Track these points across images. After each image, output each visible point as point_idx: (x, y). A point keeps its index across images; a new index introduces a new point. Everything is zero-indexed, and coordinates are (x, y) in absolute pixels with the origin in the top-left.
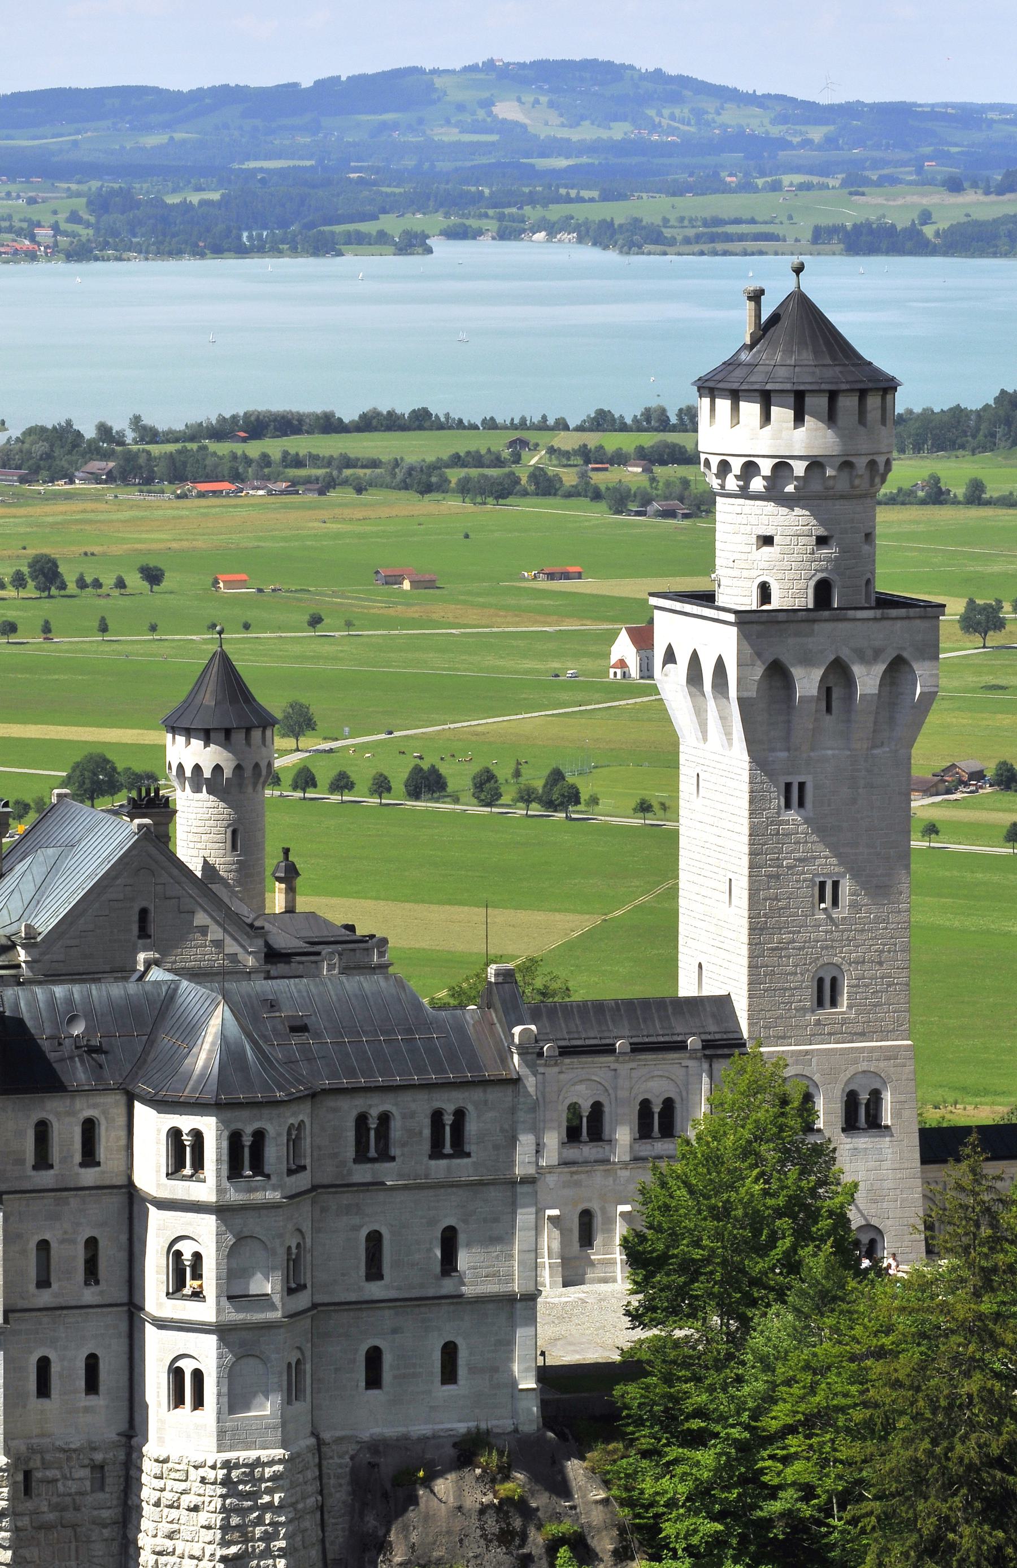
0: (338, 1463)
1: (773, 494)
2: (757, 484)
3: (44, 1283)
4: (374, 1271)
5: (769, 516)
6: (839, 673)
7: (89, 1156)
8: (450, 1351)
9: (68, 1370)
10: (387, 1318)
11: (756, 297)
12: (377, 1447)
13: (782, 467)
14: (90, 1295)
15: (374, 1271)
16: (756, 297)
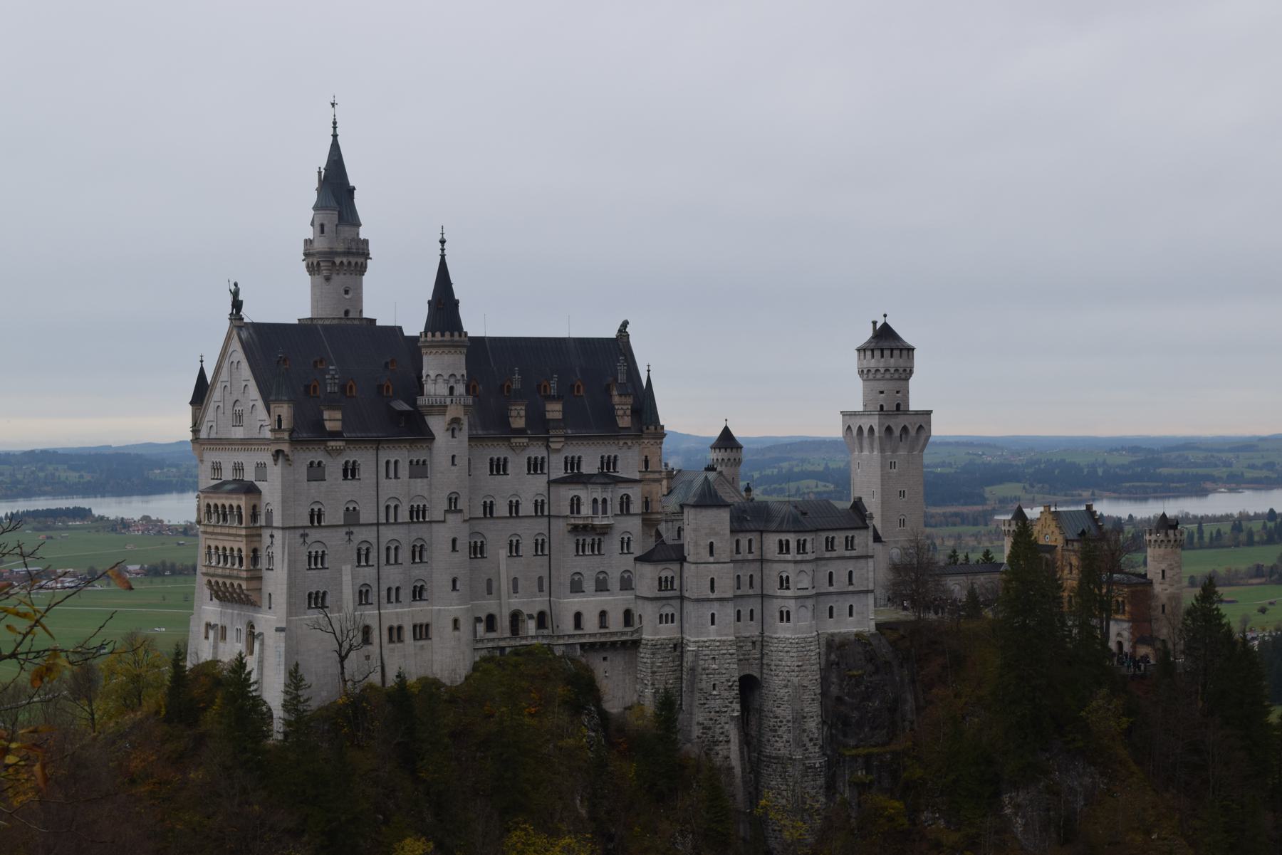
0: (823, 641)
1: (883, 379)
2: (879, 376)
3: (739, 588)
4: (831, 584)
5: (881, 385)
6: (905, 429)
7: (750, 551)
8: (851, 607)
9: (745, 614)
10: (835, 598)
11: (875, 323)
12: (832, 635)
13: (887, 370)
14: (751, 592)
15: (831, 584)
16: (875, 323)
